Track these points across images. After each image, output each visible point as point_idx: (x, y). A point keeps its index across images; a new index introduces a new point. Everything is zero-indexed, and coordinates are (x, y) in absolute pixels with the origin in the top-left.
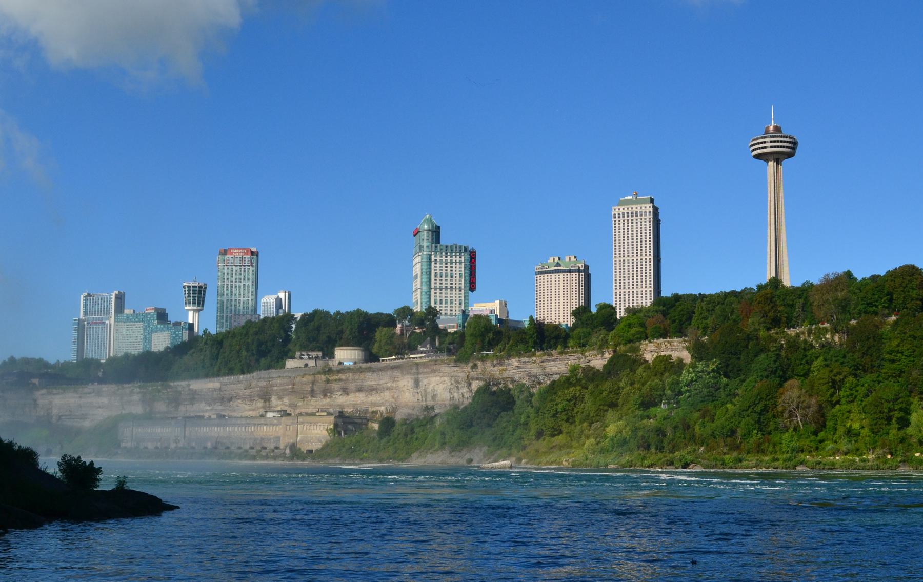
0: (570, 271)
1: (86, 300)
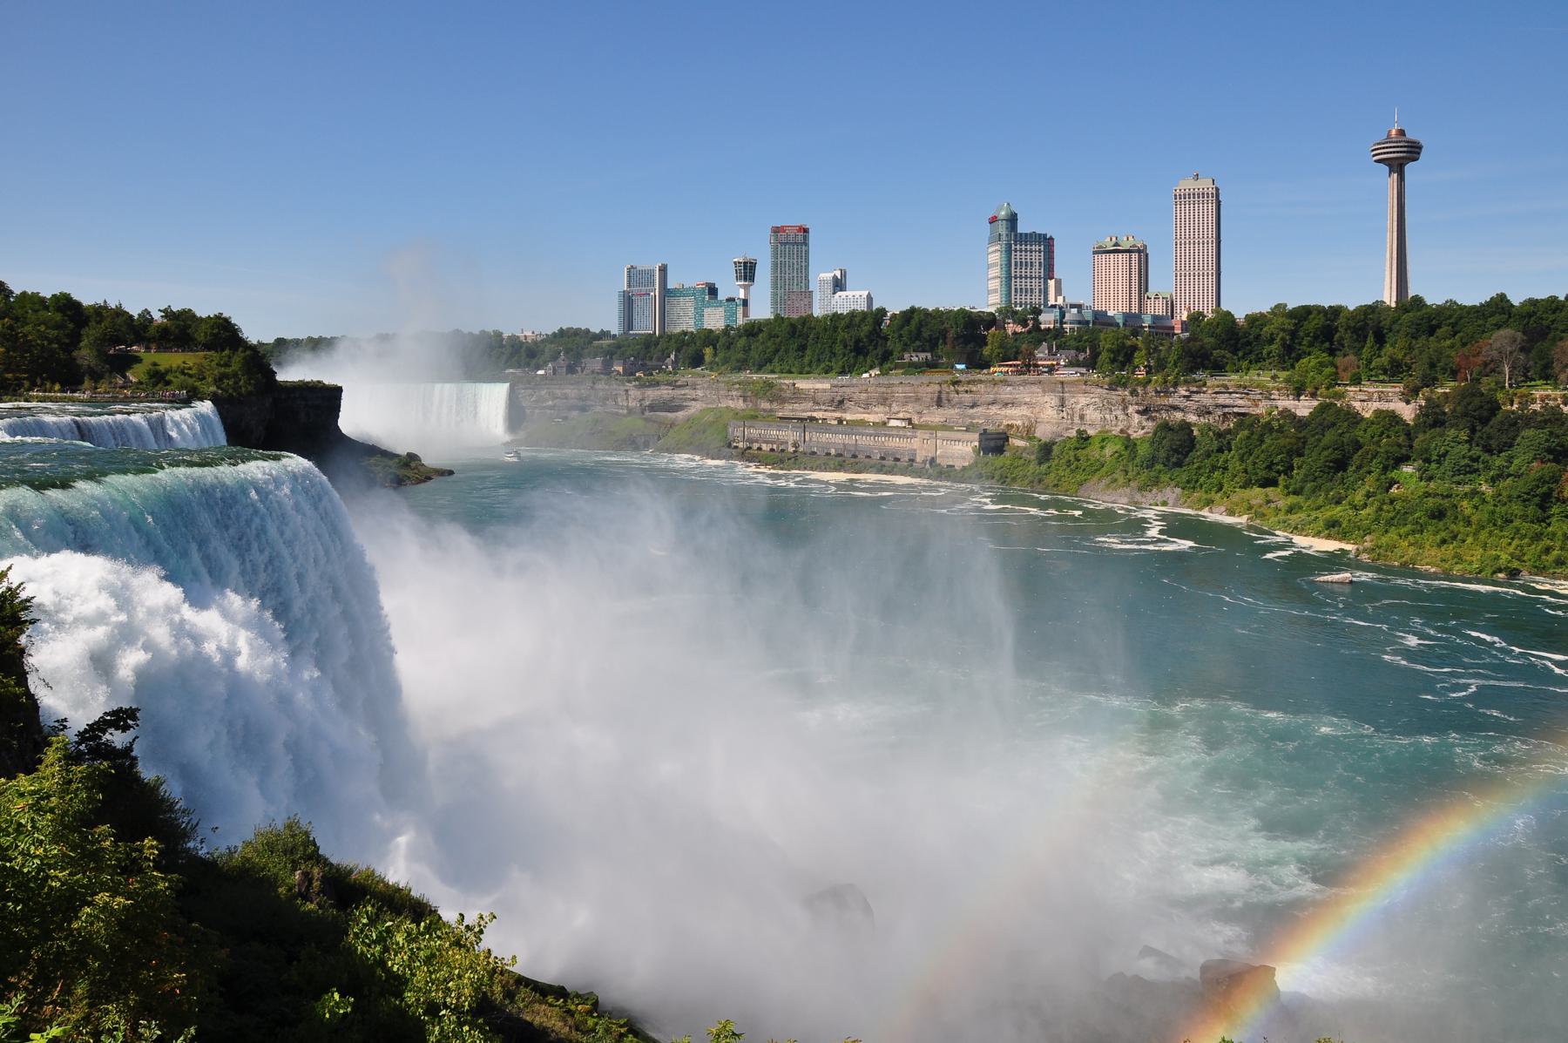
1: (629, 272)
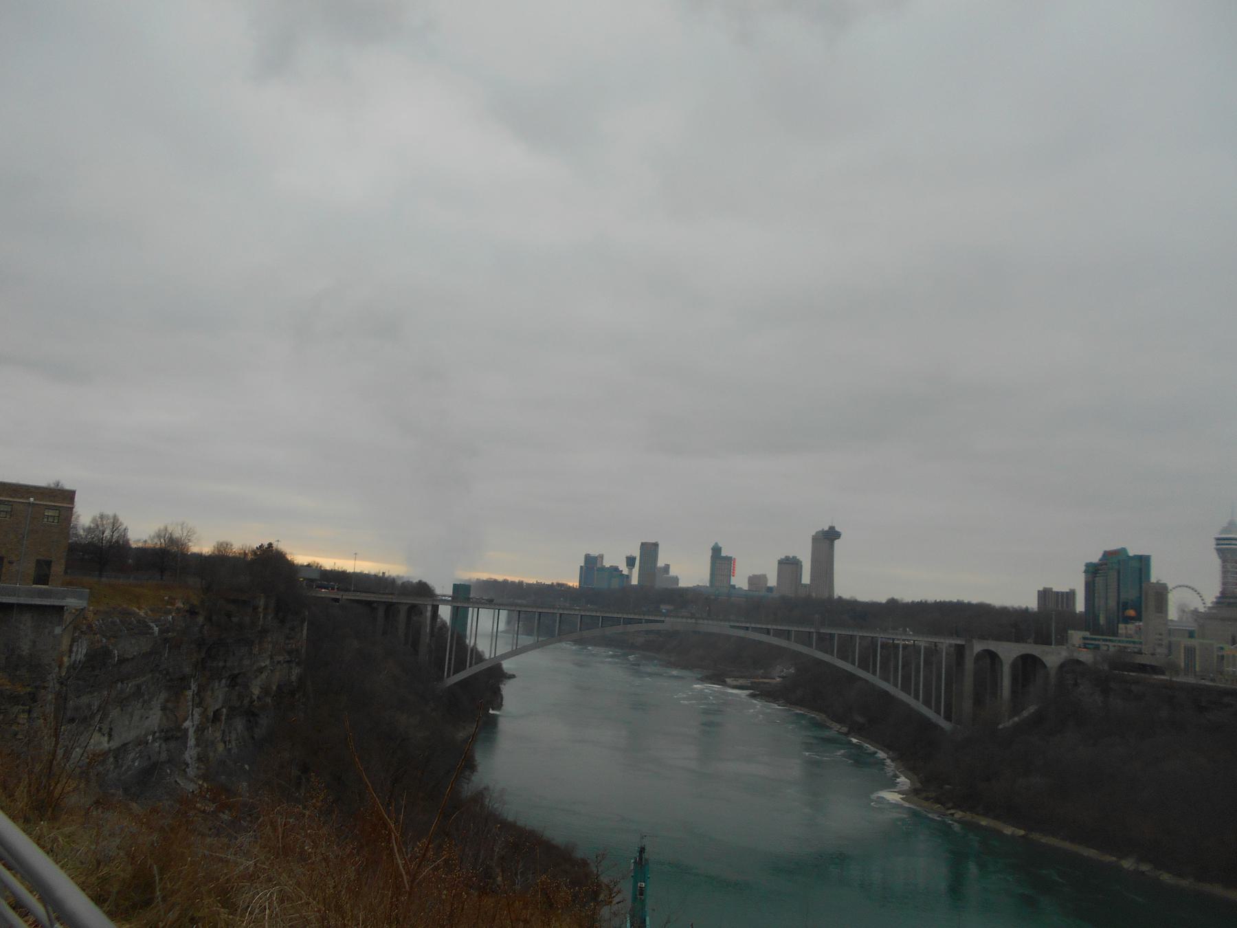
0: (792, 564)
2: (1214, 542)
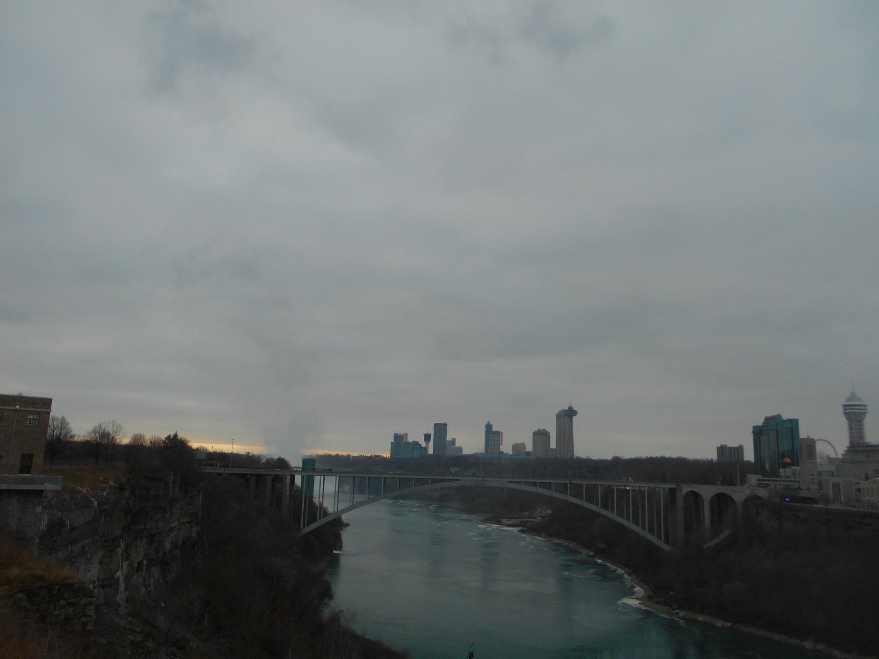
2: (841, 408)
